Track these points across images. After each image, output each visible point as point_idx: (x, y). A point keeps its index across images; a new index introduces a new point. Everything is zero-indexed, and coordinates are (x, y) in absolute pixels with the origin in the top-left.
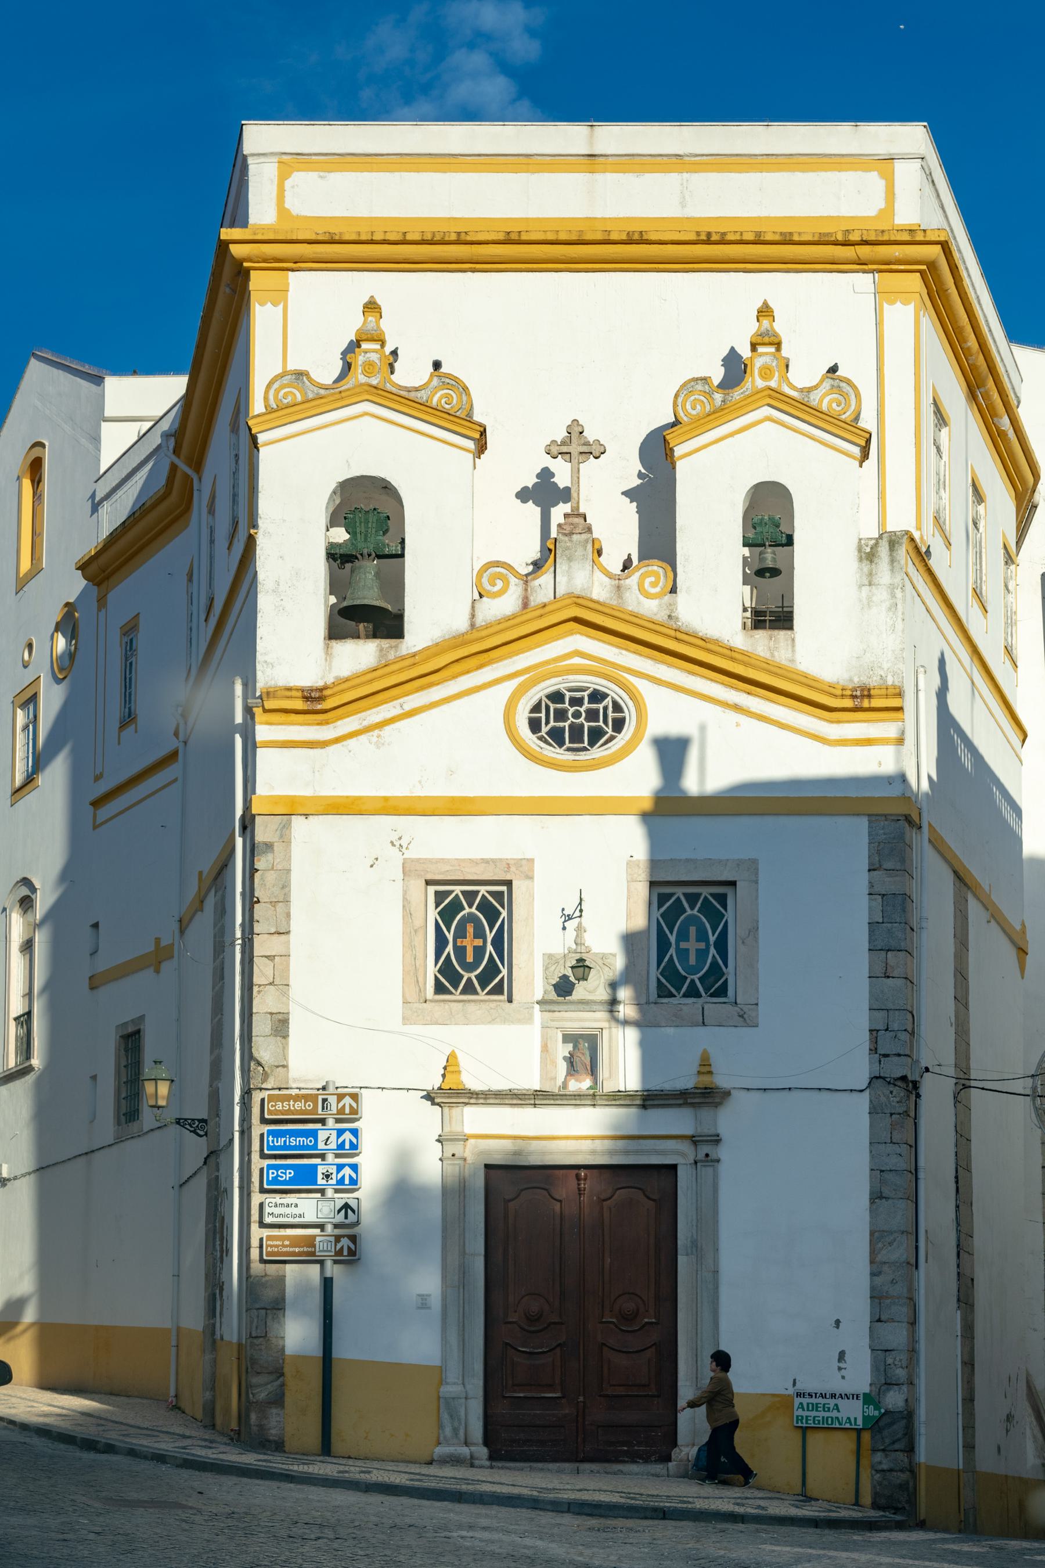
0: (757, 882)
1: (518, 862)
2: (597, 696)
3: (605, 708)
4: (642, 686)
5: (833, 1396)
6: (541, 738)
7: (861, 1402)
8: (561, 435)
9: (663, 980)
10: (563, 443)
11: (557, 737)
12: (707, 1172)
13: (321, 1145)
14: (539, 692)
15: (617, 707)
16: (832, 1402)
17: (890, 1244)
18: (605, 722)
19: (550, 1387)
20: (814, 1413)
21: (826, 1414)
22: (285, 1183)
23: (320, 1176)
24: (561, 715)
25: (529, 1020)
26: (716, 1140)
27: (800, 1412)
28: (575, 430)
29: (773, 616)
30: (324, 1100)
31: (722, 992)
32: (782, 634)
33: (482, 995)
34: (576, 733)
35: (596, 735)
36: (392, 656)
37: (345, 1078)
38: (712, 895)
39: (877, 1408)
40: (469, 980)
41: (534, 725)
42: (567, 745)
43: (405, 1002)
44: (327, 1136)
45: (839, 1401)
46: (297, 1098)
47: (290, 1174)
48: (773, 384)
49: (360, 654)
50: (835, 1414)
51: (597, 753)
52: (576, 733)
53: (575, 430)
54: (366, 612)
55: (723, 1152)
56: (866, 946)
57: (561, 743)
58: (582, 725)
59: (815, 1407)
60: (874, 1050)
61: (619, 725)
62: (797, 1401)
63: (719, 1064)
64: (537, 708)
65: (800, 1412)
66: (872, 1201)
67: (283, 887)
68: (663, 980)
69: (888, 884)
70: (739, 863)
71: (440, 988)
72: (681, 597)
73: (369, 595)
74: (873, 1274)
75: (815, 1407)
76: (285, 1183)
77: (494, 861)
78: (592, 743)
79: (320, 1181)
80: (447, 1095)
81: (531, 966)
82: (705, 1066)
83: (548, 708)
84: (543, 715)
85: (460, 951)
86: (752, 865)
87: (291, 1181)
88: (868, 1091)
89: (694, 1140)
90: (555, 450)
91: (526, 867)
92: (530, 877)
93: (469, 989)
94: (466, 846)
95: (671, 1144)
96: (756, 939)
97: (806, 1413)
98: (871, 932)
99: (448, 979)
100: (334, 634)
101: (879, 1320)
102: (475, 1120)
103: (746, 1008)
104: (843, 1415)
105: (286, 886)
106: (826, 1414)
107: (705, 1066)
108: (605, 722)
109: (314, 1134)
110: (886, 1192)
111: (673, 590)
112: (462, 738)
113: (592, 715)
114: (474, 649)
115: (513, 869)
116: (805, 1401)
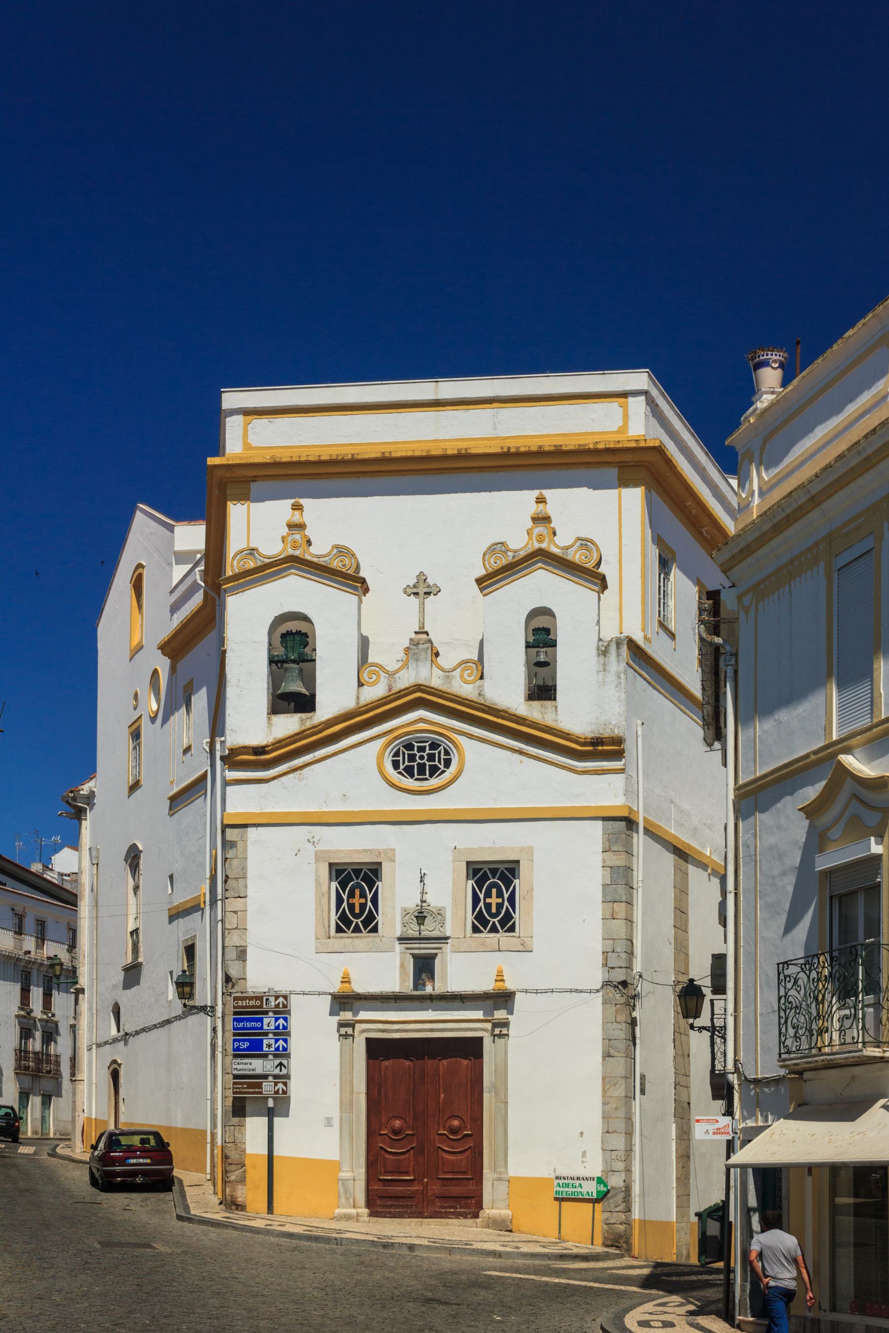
0: (532, 861)
1: (386, 851)
2: (434, 746)
3: (439, 753)
5: (578, 1179)
6: (400, 773)
7: (595, 1182)
8: (412, 581)
9: (476, 923)
10: (415, 586)
11: (409, 771)
13: (265, 1027)
16: (577, 1182)
17: (615, 1085)
18: (439, 762)
19: (407, 1173)
20: (567, 1189)
21: (574, 1190)
22: (244, 1050)
23: (265, 1046)
24: (412, 758)
25: (392, 950)
27: (558, 1189)
28: (422, 578)
30: (267, 1000)
32: (548, 703)
33: (365, 933)
35: (434, 770)
36: (308, 724)
37: (282, 987)
38: (506, 869)
39: (606, 1185)
40: (357, 923)
41: (396, 765)
42: (416, 776)
43: (317, 938)
44: (269, 1022)
45: (582, 1182)
46: (251, 998)
47: (247, 1044)
48: (544, 545)
49: (289, 724)
50: (579, 1189)
51: (434, 782)
53: (422, 578)
54: (293, 700)
56: (601, 899)
57: (412, 776)
58: (425, 764)
59: (567, 1185)
60: (605, 965)
61: (448, 763)
62: (556, 1181)
64: (397, 754)
65: (558, 1189)
66: (604, 1058)
67: (243, 869)
68: (476, 923)
70: (522, 849)
71: (339, 930)
72: (486, 682)
73: (296, 686)
74: (604, 1104)
75: (567, 1185)
76: (244, 1050)
77: (370, 850)
78: (431, 776)
79: (265, 1049)
83: (404, 753)
84: (401, 758)
85: (351, 907)
87: (247, 1049)
90: (409, 591)
93: (357, 930)
94: (353, 845)
96: (532, 897)
97: (560, 1189)
98: (604, 891)
99: (344, 924)
101: (608, 1132)
103: (525, 940)
104: (584, 1190)
105: (244, 868)
106: (574, 1190)
108: (439, 762)
109: (261, 1020)
110: (612, 1052)
111: (482, 678)
113: (431, 757)
115: (382, 855)
116: (561, 1182)
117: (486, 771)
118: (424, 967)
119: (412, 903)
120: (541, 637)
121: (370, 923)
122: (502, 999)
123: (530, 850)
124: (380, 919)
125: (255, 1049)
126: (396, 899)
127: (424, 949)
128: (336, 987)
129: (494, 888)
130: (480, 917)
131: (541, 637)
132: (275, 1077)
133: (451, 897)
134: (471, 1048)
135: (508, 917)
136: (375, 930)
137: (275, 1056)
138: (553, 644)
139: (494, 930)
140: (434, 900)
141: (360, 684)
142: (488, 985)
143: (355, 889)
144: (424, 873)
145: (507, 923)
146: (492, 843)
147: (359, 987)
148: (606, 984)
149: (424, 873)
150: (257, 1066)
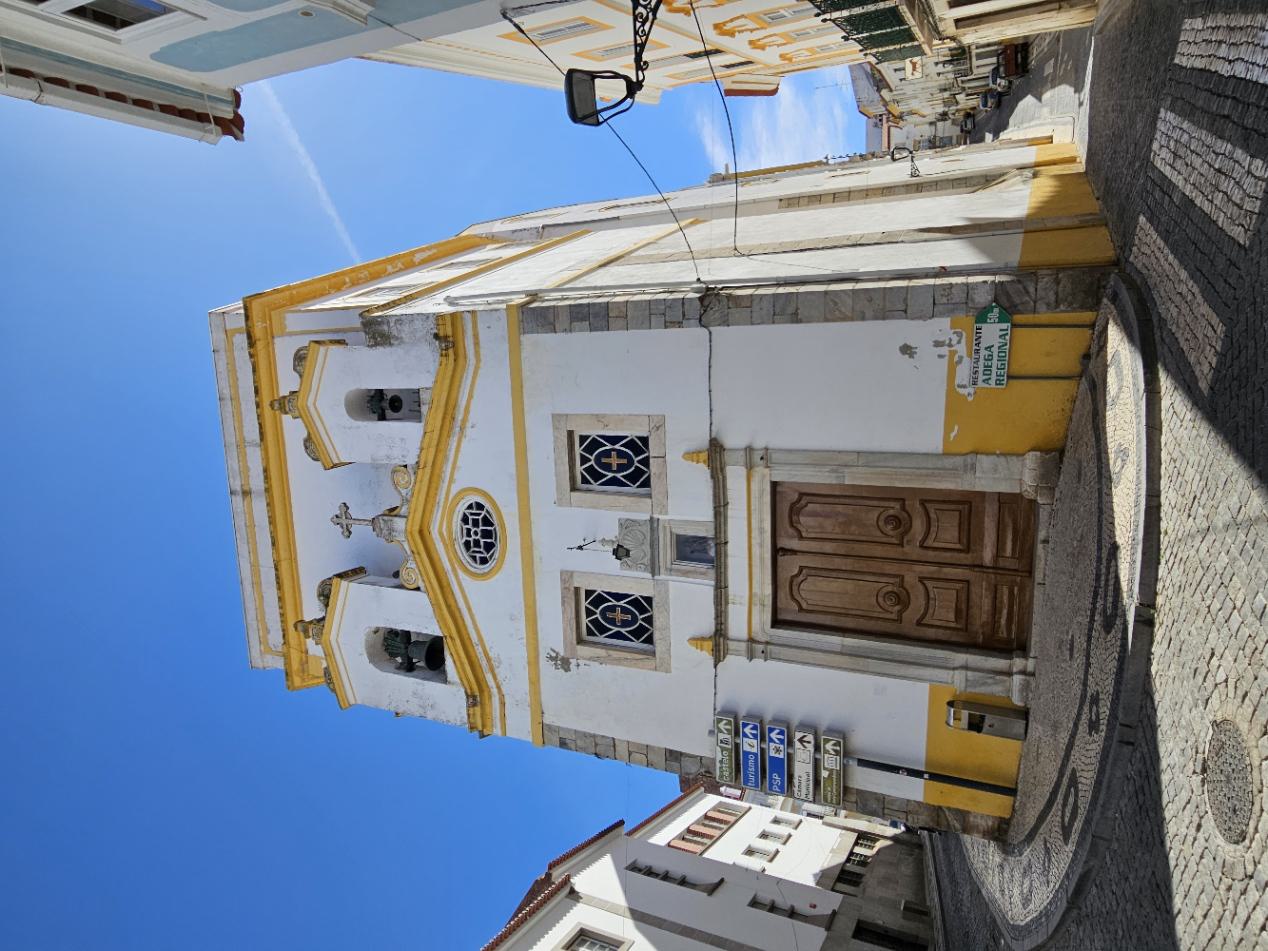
0: (567, 415)
1: (563, 581)
2: (465, 520)
3: (472, 514)
4: (454, 490)
5: (977, 351)
6: (491, 557)
7: (984, 326)
9: (638, 484)
10: (342, 527)
11: (489, 547)
12: (775, 456)
13: (754, 750)
15: (470, 507)
16: (983, 353)
17: (836, 304)
18: (479, 514)
20: (994, 369)
21: (995, 358)
22: (782, 782)
23: (777, 755)
25: (665, 583)
26: (749, 450)
27: (992, 382)
30: (721, 742)
31: (645, 440)
34: (487, 534)
35: (487, 522)
38: (580, 446)
39: (991, 309)
41: (484, 561)
42: (493, 541)
43: (656, 669)
45: (983, 346)
47: (776, 776)
50: (995, 350)
51: (495, 520)
55: (759, 444)
56: (606, 332)
58: (482, 530)
59: (988, 368)
60: (680, 324)
61: (480, 506)
62: (980, 384)
63: (694, 445)
64: (474, 558)
65: (992, 382)
66: (799, 321)
68: (638, 484)
69: (564, 318)
70: (556, 428)
74: (863, 318)
75: (988, 368)
76: (782, 782)
77: (563, 598)
78: (492, 525)
79: (781, 756)
81: (632, 582)
82: (692, 455)
83: (474, 552)
84: (478, 555)
85: (625, 624)
86: (557, 418)
87: (781, 776)
88: (711, 328)
89: (750, 467)
90: (347, 533)
91: (566, 576)
92: (571, 574)
95: (755, 487)
96: (604, 416)
97: (994, 377)
98: (596, 329)
101: (905, 311)
103: (652, 425)
104: (996, 342)
106: (995, 358)
107: (692, 455)
108: (479, 514)
109: (746, 754)
110: (790, 310)
113: (476, 523)
115: (567, 585)
116: (981, 377)
117: (480, 465)
121: (643, 605)
122: (715, 453)
128: (707, 657)
129: (614, 462)
130: (633, 478)
132: (817, 748)
133: (608, 513)
135: (631, 444)
137: (790, 743)
138: (380, 393)
139: (646, 462)
140: (613, 532)
141: (418, 589)
142: (702, 471)
143: (618, 621)
145: (639, 446)
146: (548, 463)
147: (708, 626)
148: (701, 323)
149: (573, 539)
150: (802, 769)
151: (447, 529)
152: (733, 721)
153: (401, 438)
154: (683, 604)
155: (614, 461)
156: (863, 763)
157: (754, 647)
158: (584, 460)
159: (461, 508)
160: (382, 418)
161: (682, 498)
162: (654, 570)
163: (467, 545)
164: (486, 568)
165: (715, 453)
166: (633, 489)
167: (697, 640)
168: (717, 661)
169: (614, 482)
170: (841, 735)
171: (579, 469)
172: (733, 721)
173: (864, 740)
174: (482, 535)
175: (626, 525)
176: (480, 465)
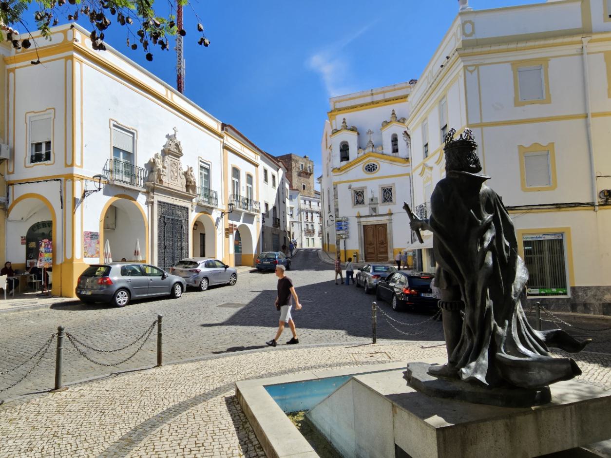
2: (374, 164)
4: (379, 162)
11: (369, 170)
14: (367, 164)
24: (369, 167)
26: (391, 220)
29: (396, 150)
34: (371, 169)
35: (374, 169)
41: (366, 169)
51: (374, 172)
52: (371, 169)
55: (393, 221)
61: (377, 168)
80: (359, 217)
81: (367, 201)
82: (390, 210)
89: (389, 220)
91: (366, 187)
100: (342, 160)
102: (362, 220)
107: (390, 210)
111: (383, 149)
112: (357, 172)
113: (373, 167)
114: (358, 161)
118: (374, 210)
119: (371, 197)
120: (395, 140)
121: (363, 202)
123: (394, 184)
124: (365, 201)
125: (341, 229)
126: (368, 196)
127: (373, 206)
128: (357, 215)
131: (395, 140)
133: (378, 195)
134: (384, 226)
136: (364, 203)
140: (375, 196)
142: (387, 212)
143: (359, 197)
144: (373, 190)
146: (386, 183)
147: (362, 215)
149: (373, 190)
150: (341, 232)
151: (371, 160)
152: (347, 220)
153: (388, 148)
154: (364, 210)
155: (388, 195)
156: (345, 241)
157: (359, 223)
158: (387, 189)
159: (376, 164)
160: (392, 141)
161: (383, 209)
162: (370, 204)
163: (369, 165)
164: (365, 170)
165: (391, 214)
166: (383, 199)
167: (359, 213)
168: (356, 217)
169: (384, 195)
170: (348, 237)
171: (386, 188)
172: (347, 220)
173: (348, 241)
174: (371, 168)
175: (377, 198)
176: (385, 167)
